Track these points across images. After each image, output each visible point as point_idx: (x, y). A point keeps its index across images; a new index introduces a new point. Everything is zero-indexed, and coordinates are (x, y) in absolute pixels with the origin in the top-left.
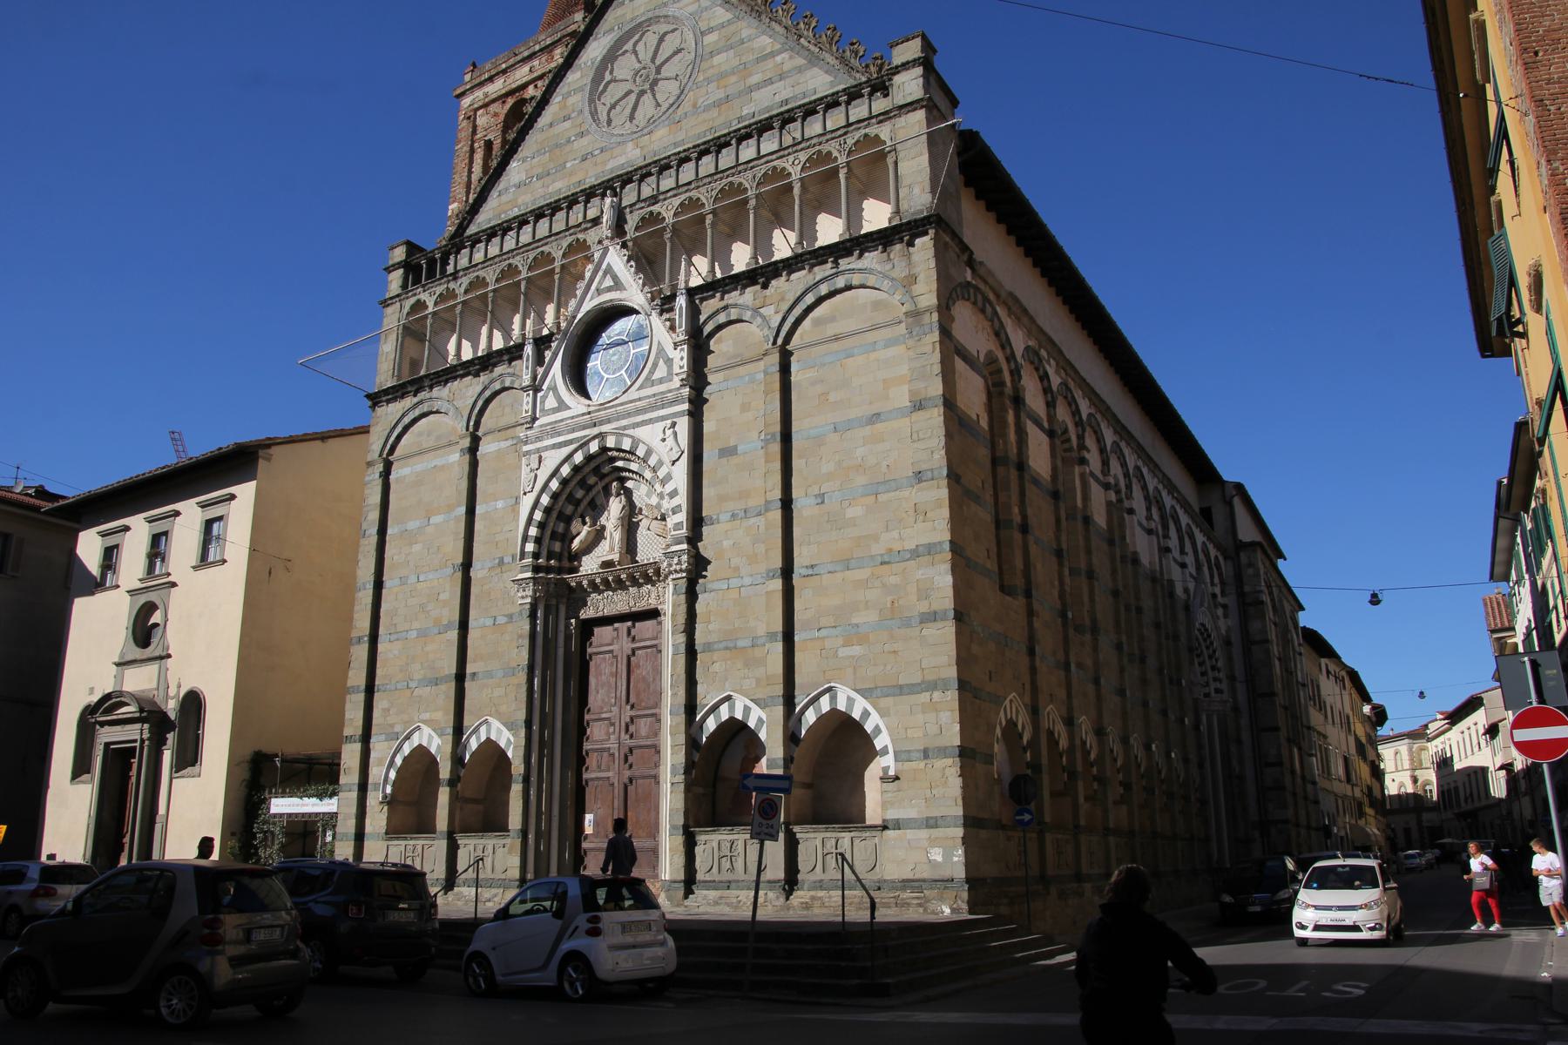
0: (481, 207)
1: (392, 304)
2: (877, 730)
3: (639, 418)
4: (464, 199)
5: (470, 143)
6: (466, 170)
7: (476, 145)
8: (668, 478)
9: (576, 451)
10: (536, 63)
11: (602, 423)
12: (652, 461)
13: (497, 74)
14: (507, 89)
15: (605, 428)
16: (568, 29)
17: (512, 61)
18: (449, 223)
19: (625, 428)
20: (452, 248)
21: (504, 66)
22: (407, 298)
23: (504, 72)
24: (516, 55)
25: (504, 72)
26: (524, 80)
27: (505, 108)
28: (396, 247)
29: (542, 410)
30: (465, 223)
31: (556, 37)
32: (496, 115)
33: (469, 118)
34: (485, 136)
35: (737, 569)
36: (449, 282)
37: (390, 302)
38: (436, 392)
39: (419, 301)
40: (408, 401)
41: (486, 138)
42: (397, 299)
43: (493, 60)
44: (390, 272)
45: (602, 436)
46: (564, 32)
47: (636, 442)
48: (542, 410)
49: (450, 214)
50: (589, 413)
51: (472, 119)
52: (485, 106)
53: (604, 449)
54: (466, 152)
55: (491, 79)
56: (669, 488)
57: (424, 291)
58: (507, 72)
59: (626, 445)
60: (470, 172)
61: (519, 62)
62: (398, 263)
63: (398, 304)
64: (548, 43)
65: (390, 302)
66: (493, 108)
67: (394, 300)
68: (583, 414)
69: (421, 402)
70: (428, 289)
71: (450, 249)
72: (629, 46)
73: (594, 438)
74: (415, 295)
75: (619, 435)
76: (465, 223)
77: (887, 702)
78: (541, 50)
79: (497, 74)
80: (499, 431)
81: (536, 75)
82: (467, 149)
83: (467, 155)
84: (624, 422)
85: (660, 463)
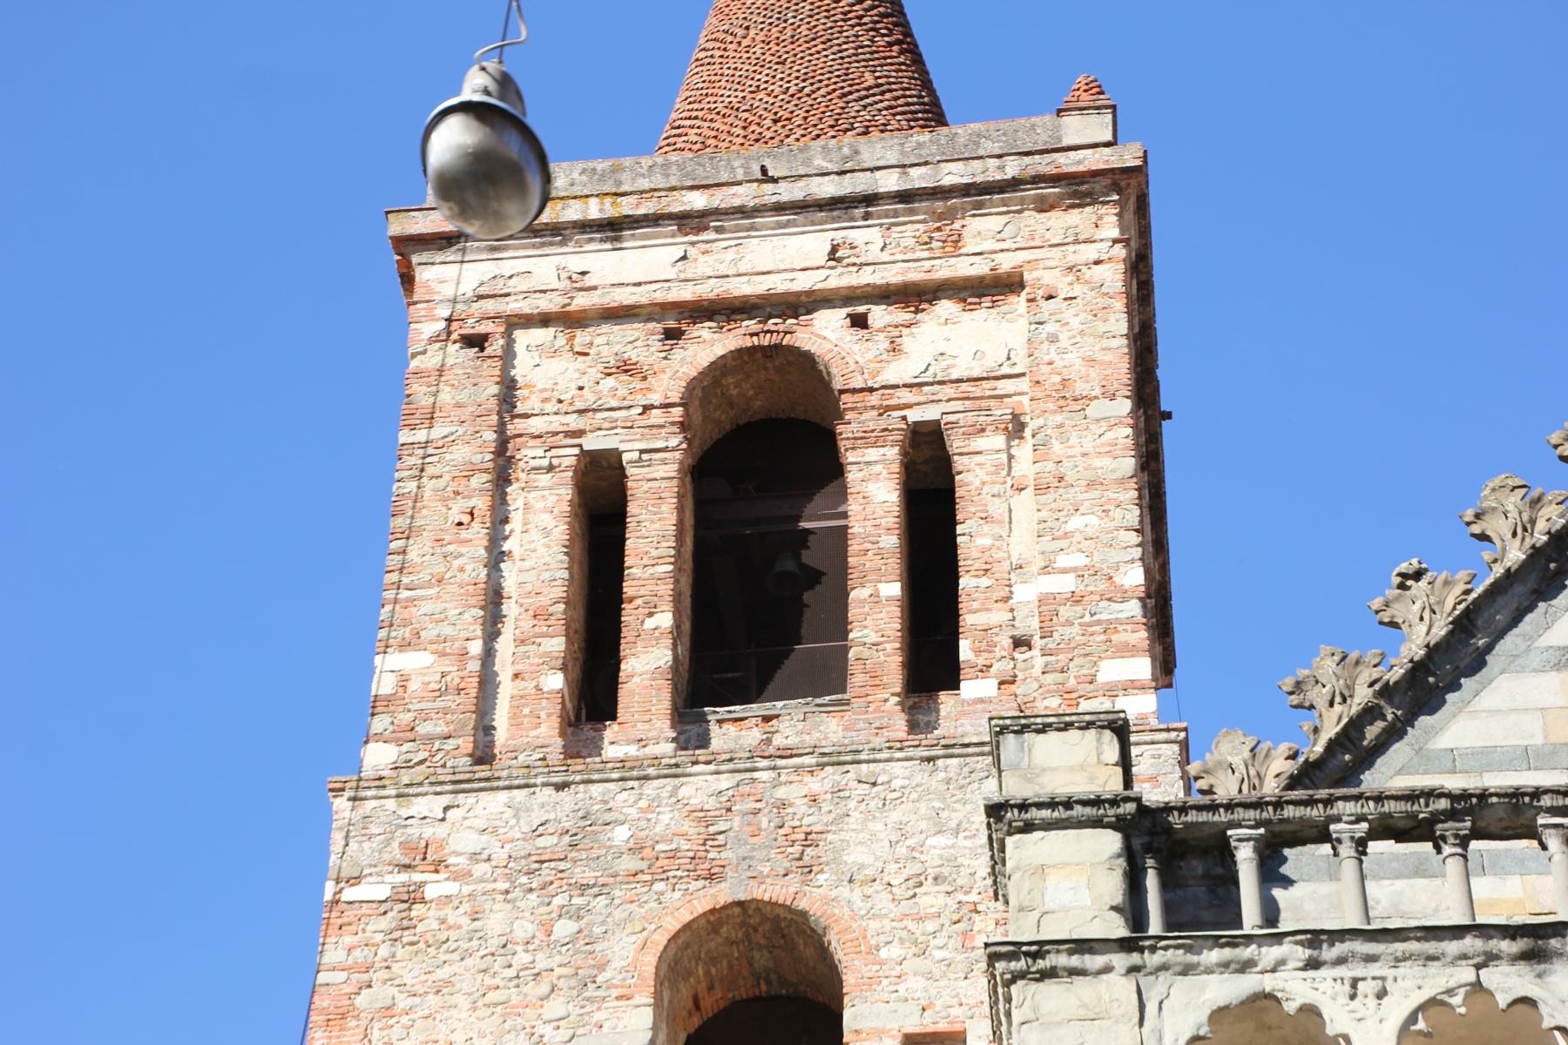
0: (1455, 686)
1: (1074, 972)
4: (476, 648)
5: (490, 436)
6: (478, 533)
7: (529, 454)
10: (866, 237)
13: (654, 220)
14: (708, 290)
16: (1061, 158)
17: (744, 195)
18: (379, 724)
20: (1452, 815)
21: (697, 201)
22: (1187, 970)
23: (690, 222)
24: (766, 177)
25: (690, 222)
26: (804, 282)
27: (677, 354)
28: (1043, 729)
30: (1372, 731)
31: (991, 171)
32: (625, 368)
33: (476, 342)
34: (579, 433)
36: (1490, 958)
37: (1063, 960)
39: (1265, 1000)
41: (592, 443)
42: (1120, 960)
43: (601, 165)
44: (1028, 828)
46: (1043, 165)
49: (384, 685)
51: (495, 346)
52: (570, 320)
54: (471, 470)
55: (612, 229)
57: (1313, 964)
58: (706, 228)
60: (496, 557)
61: (779, 208)
62: (1096, 802)
63: (1118, 988)
64: (947, 181)
65: (1063, 960)
66: (611, 340)
67: (1095, 961)
70: (1341, 961)
71: (1436, 818)
74: (1245, 967)
76: (1372, 731)
78: (905, 197)
79: (654, 220)
81: (867, 277)
82: (476, 450)
83: (480, 480)
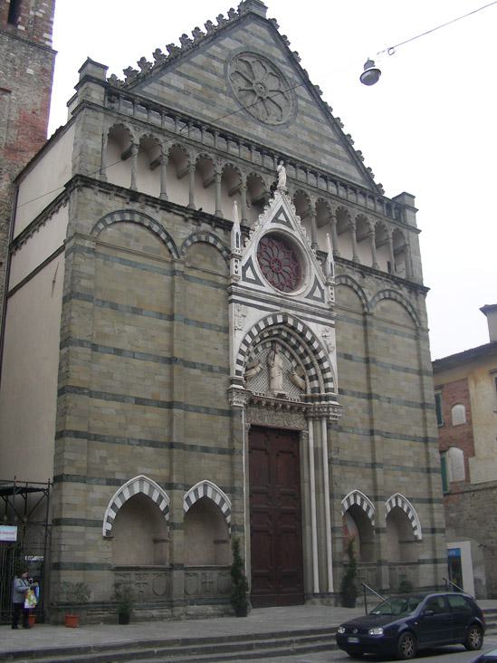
2: (413, 518)
3: (309, 316)
8: (325, 359)
9: (269, 316)
11: (286, 307)
12: (315, 345)
15: (291, 312)
19: (301, 317)
29: (244, 275)
35: (356, 424)
38: (149, 211)
40: (116, 204)
45: (285, 316)
47: (306, 328)
48: (244, 275)
50: (278, 296)
53: (285, 323)
56: (326, 365)
59: (300, 328)
68: (272, 294)
69: (131, 212)
72: (269, 70)
73: (280, 314)
75: (296, 321)
77: (417, 505)
80: (204, 271)
84: (300, 314)
85: (320, 348)
